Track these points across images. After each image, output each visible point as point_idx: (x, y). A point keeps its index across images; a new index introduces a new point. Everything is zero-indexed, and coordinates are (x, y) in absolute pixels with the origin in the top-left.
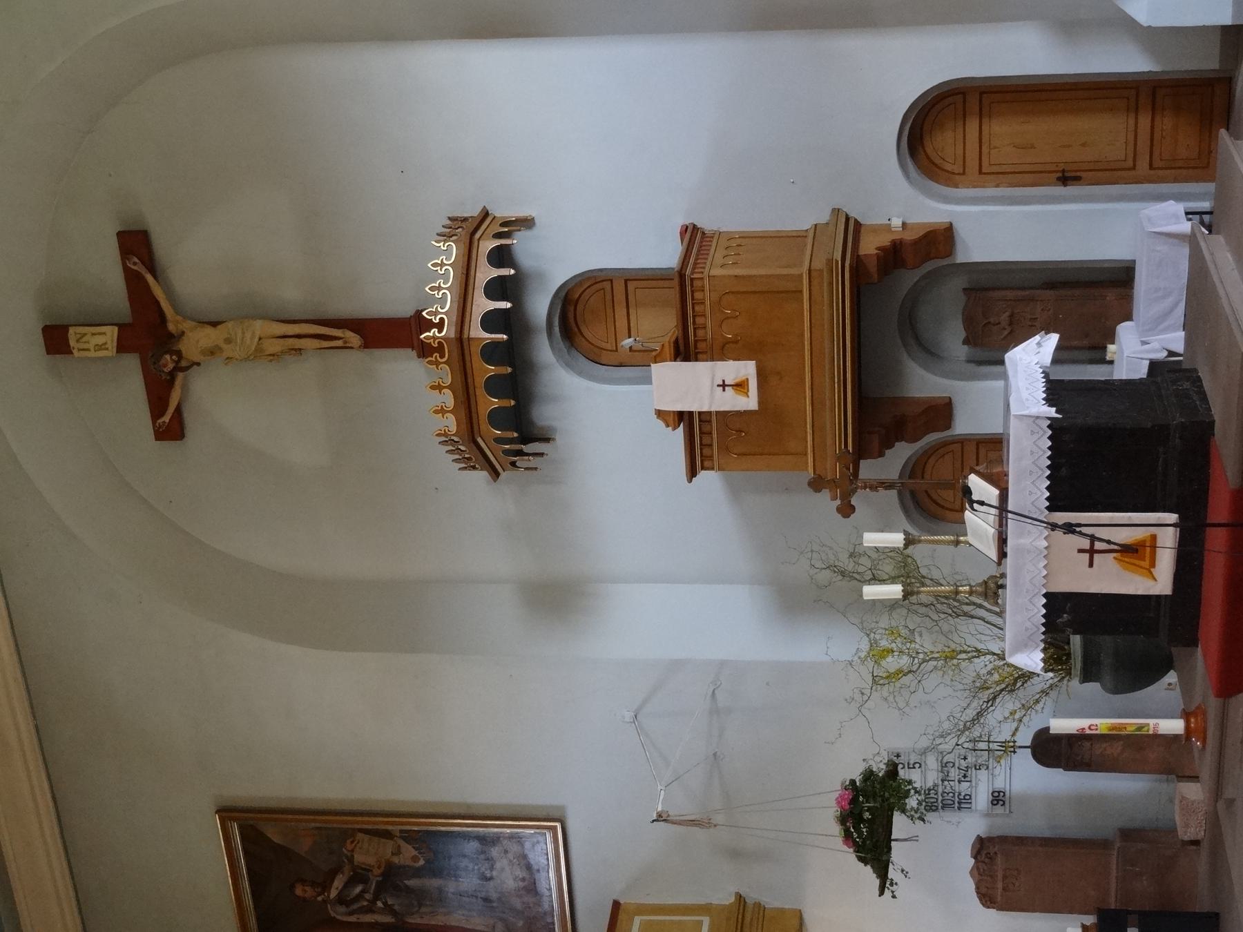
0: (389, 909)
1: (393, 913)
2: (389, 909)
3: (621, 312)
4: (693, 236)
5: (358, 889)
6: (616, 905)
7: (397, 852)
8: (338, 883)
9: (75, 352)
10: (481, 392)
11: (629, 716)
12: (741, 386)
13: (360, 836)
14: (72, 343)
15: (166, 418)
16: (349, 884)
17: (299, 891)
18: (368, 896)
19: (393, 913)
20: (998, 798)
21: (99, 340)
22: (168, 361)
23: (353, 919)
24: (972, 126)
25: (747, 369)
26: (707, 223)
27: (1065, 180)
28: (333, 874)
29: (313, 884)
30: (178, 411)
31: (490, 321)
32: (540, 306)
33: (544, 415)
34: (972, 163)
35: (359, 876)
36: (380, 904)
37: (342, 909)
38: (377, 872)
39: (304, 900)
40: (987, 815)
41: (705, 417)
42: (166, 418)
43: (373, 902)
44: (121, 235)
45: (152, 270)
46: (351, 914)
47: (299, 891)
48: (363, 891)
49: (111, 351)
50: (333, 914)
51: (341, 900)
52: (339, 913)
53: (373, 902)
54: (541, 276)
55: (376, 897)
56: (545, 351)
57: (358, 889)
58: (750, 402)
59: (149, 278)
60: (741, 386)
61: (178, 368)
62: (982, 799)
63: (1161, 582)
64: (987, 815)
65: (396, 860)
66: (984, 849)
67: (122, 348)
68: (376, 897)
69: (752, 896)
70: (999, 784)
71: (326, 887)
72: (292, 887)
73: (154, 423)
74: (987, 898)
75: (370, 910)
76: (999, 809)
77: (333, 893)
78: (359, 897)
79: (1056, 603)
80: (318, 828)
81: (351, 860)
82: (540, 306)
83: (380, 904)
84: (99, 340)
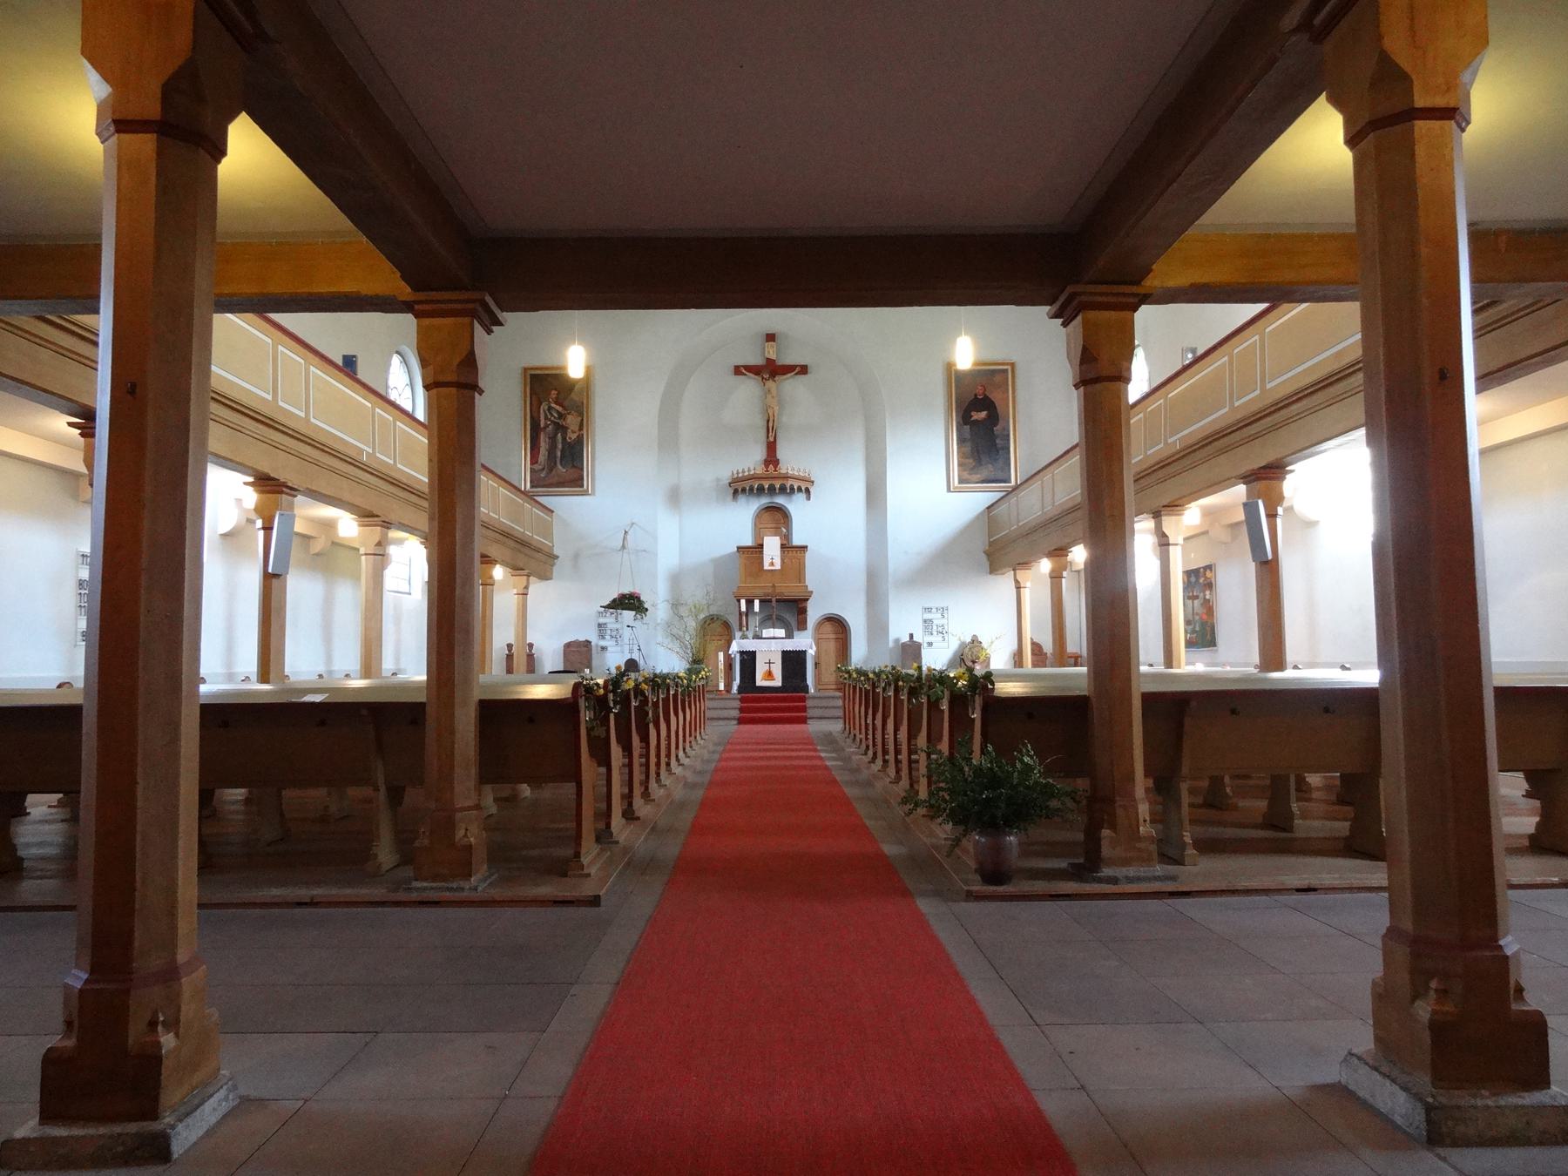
0: (547, 426)
1: (545, 428)
2: (547, 426)
3: (774, 525)
4: (805, 548)
5: (556, 415)
6: (553, 512)
7: (573, 432)
8: (558, 407)
9: (767, 344)
10: (770, 482)
11: (634, 521)
12: (772, 564)
13: (580, 418)
14: (770, 343)
15: (744, 371)
16: (558, 412)
17: (553, 392)
18: (552, 418)
19: (545, 428)
20: (604, 648)
21: (771, 352)
22: (767, 376)
23: (542, 411)
24: (833, 636)
25: (778, 566)
26: (808, 554)
27: (816, 664)
28: (561, 405)
29: (557, 398)
30: (745, 375)
31: (792, 488)
32: (780, 500)
33: (742, 499)
34: (821, 636)
35: (561, 416)
36: (549, 423)
37: (546, 407)
38: (564, 423)
39: (550, 394)
40: (597, 646)
41: (762, 552)
42: (744, 371)
43: (550, 420)
44: (807, 366)
45: (796, 374)
46: (544, 411)
47: (553, 392)
48: (555, 417)
49: (767, 355)
50: (543, 404)
51: (550, 408)
52: (544, 406)
53: (550, 420)
54: (791, 501)
55: (552, 421)
56: (764, 501)
57: (556, 415)
58: (767, 567)
59: (793, 374)
60: (772, 564)
61: (763, 378)
62: (603, 643)
63: (760, 682)
64: (597, 646)
65: (569, 431)
66: (588, 643)
67: (768, 359)
68: (552, 421)
69: (558, 562)
70: (609, 649)
71: (556, 403)
72: (556, 390)
73: (742, 366)
74: (568, 646)
75: (546, 418)
76: (599, 649)
77: (553, 405)
78: (552, 415)
79: (754, 653)
80: (583, 403)
81: (569, 414)
82: (780, 500)
83: (549, 423)
84: (771, 352)
